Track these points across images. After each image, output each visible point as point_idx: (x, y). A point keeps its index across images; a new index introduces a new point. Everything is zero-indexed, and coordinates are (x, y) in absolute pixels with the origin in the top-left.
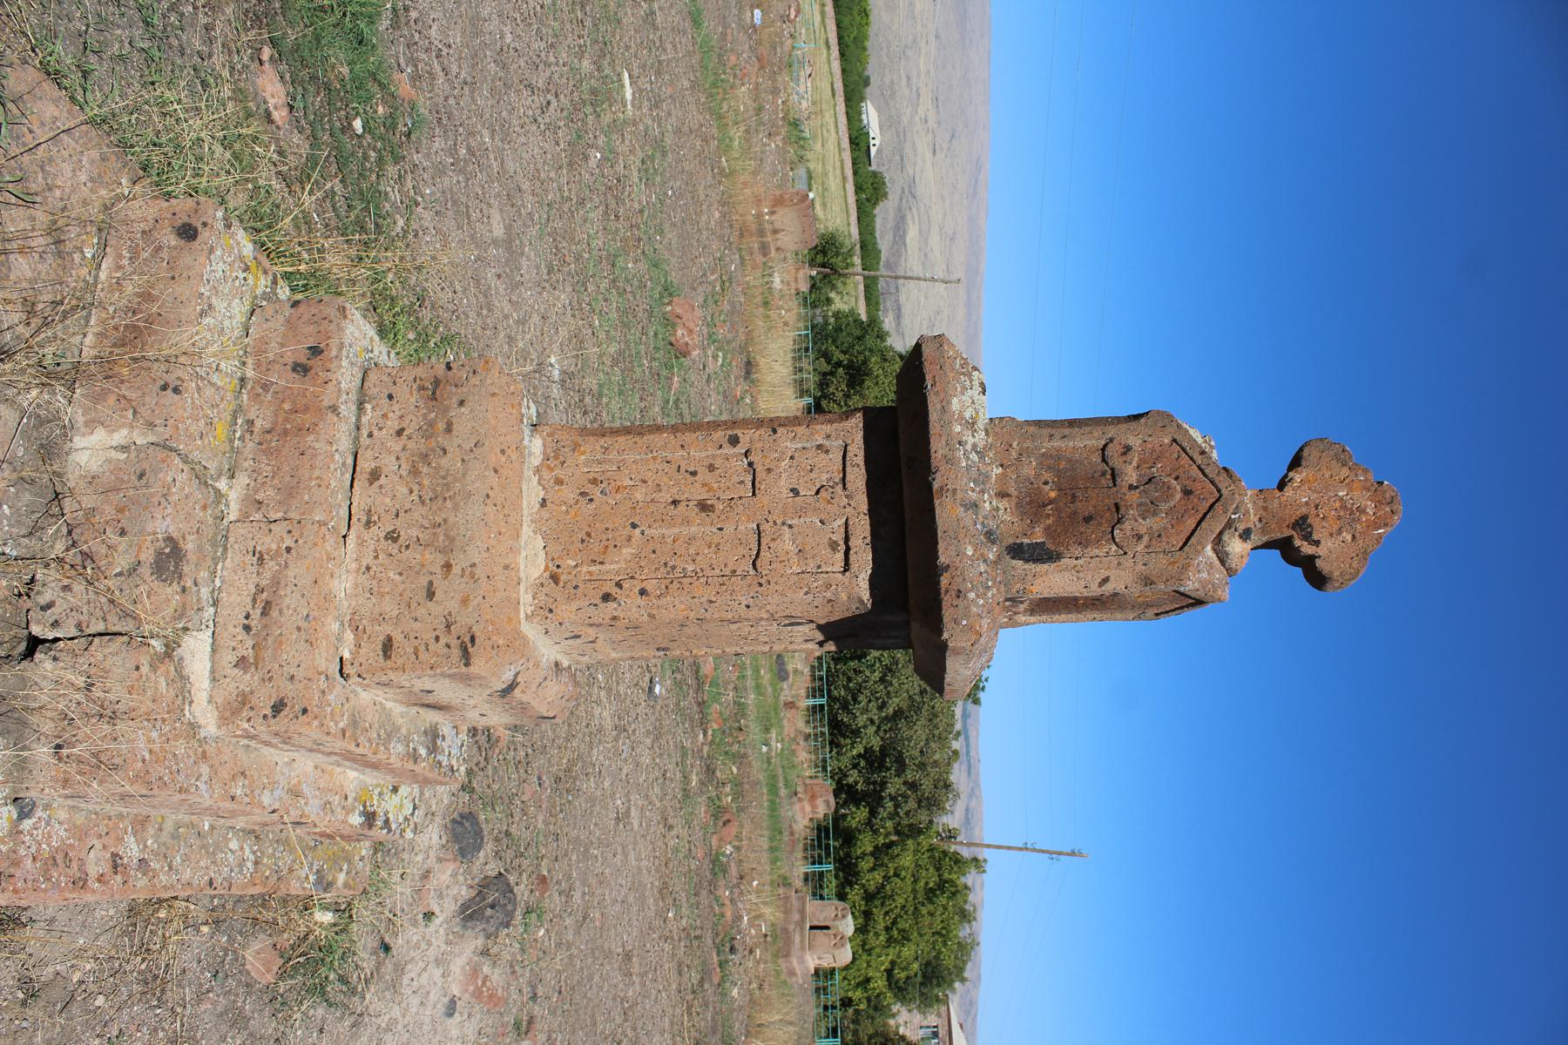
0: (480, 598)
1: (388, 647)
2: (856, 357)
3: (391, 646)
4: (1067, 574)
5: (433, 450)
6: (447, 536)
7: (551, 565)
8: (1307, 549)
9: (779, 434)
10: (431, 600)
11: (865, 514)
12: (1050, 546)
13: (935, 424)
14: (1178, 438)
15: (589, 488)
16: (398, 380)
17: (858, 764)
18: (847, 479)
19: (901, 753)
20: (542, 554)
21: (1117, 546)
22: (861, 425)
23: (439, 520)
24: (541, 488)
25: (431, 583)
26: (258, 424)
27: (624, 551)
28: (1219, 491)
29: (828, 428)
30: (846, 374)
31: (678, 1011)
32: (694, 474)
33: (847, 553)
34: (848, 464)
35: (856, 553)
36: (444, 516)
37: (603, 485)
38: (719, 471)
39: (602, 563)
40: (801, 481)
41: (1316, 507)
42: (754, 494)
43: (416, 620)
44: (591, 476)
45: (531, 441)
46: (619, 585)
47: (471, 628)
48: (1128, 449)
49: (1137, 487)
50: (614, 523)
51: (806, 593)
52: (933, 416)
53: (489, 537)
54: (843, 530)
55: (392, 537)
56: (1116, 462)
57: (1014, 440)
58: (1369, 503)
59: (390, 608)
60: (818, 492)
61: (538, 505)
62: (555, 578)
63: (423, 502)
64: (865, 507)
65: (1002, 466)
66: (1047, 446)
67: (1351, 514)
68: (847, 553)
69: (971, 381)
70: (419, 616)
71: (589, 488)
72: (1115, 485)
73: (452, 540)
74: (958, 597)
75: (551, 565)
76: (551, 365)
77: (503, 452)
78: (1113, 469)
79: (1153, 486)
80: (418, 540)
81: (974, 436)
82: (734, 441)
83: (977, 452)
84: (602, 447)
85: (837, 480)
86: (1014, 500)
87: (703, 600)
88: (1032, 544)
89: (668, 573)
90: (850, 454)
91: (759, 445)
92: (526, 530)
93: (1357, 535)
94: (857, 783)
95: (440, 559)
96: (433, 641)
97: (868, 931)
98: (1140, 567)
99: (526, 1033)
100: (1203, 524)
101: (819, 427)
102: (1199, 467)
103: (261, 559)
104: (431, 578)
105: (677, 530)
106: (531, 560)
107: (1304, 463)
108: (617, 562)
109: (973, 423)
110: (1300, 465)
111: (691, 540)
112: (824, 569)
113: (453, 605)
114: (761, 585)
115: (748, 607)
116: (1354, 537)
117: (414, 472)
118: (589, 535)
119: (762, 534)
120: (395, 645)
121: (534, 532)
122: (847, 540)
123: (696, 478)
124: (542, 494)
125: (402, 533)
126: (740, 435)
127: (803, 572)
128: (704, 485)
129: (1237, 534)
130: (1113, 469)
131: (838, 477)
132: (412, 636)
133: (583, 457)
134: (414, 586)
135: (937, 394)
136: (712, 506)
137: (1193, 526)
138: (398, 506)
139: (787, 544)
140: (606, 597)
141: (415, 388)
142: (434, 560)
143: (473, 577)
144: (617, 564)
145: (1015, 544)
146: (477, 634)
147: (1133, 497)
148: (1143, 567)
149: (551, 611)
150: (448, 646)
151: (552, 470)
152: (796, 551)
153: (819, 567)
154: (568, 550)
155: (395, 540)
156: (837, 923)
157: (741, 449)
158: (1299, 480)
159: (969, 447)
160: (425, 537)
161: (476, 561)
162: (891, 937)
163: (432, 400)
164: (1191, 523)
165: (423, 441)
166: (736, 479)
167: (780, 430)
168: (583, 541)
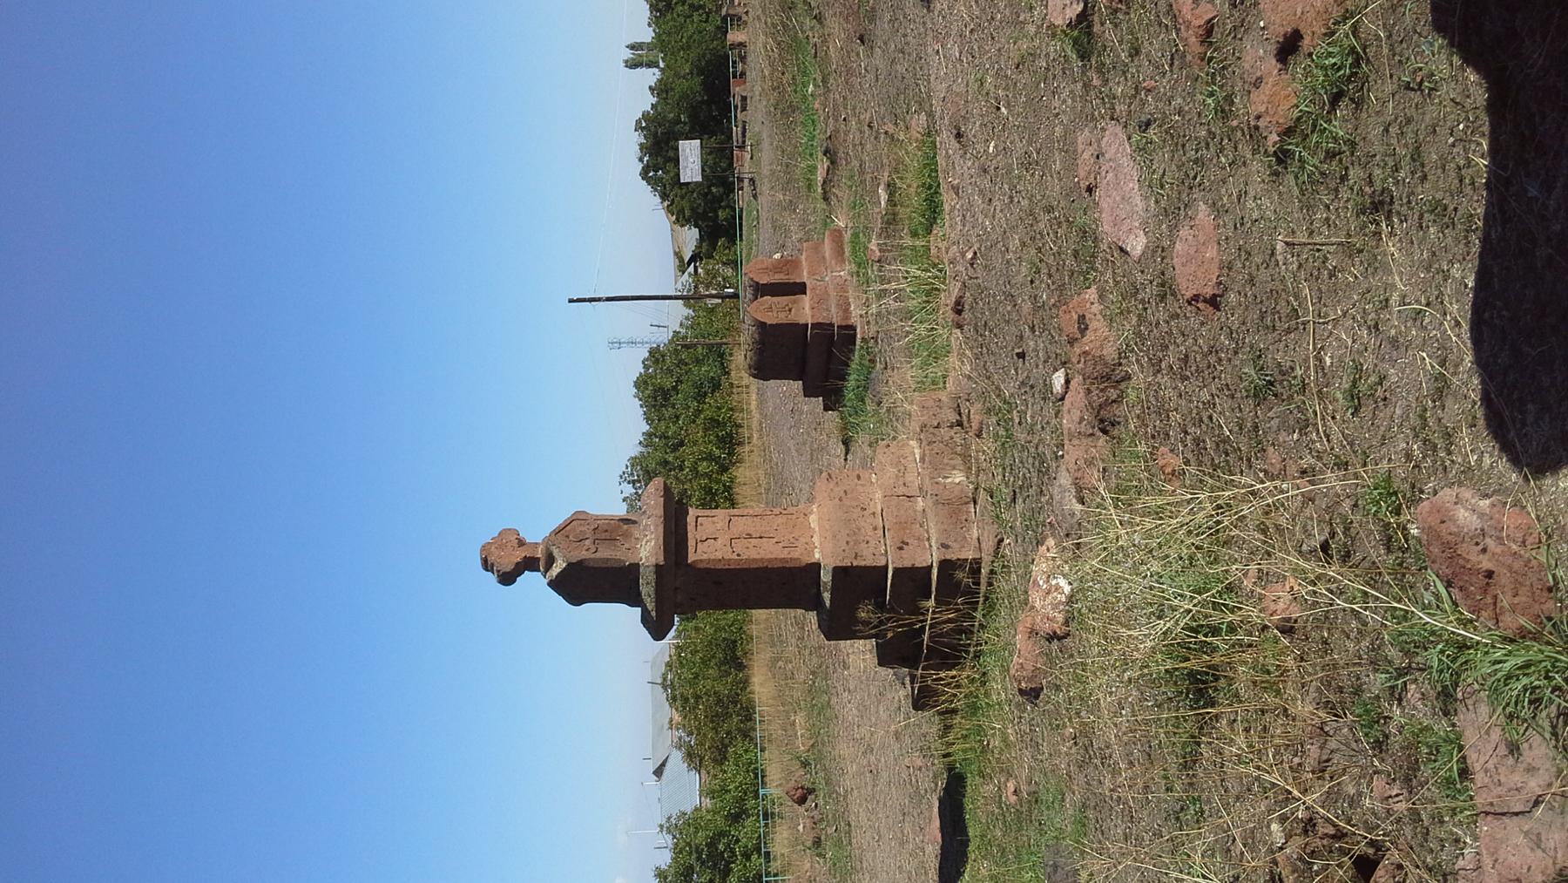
12: (621, 524)
15: (795, 542)
26: (918, 526)
29: (702, 558)
48: (587, 550)
52: (662, 538)
59: (860, 489)
64: (689, 534)
82: (738, 555)
92: (817, 529)
103: (904, 484)
106: (813, 519)
117: (859, 530)
122: (696, 526)
131: (699, 544)
142: (847, 502)
155: (862, 508)
164: (568, 527)
167: (720, 557)
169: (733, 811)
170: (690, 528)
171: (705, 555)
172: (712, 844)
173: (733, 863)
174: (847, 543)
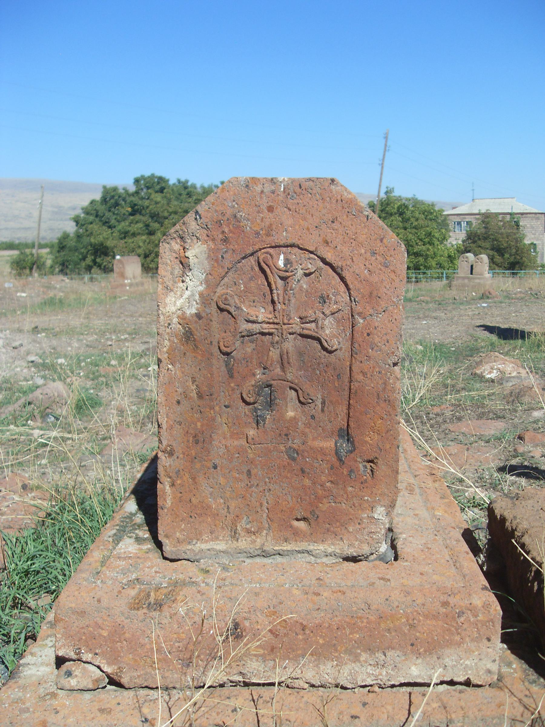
2: (89, 251)
30: (100, 257)
97: (427, 255)
156: (470, 261)
162: (429, 243)
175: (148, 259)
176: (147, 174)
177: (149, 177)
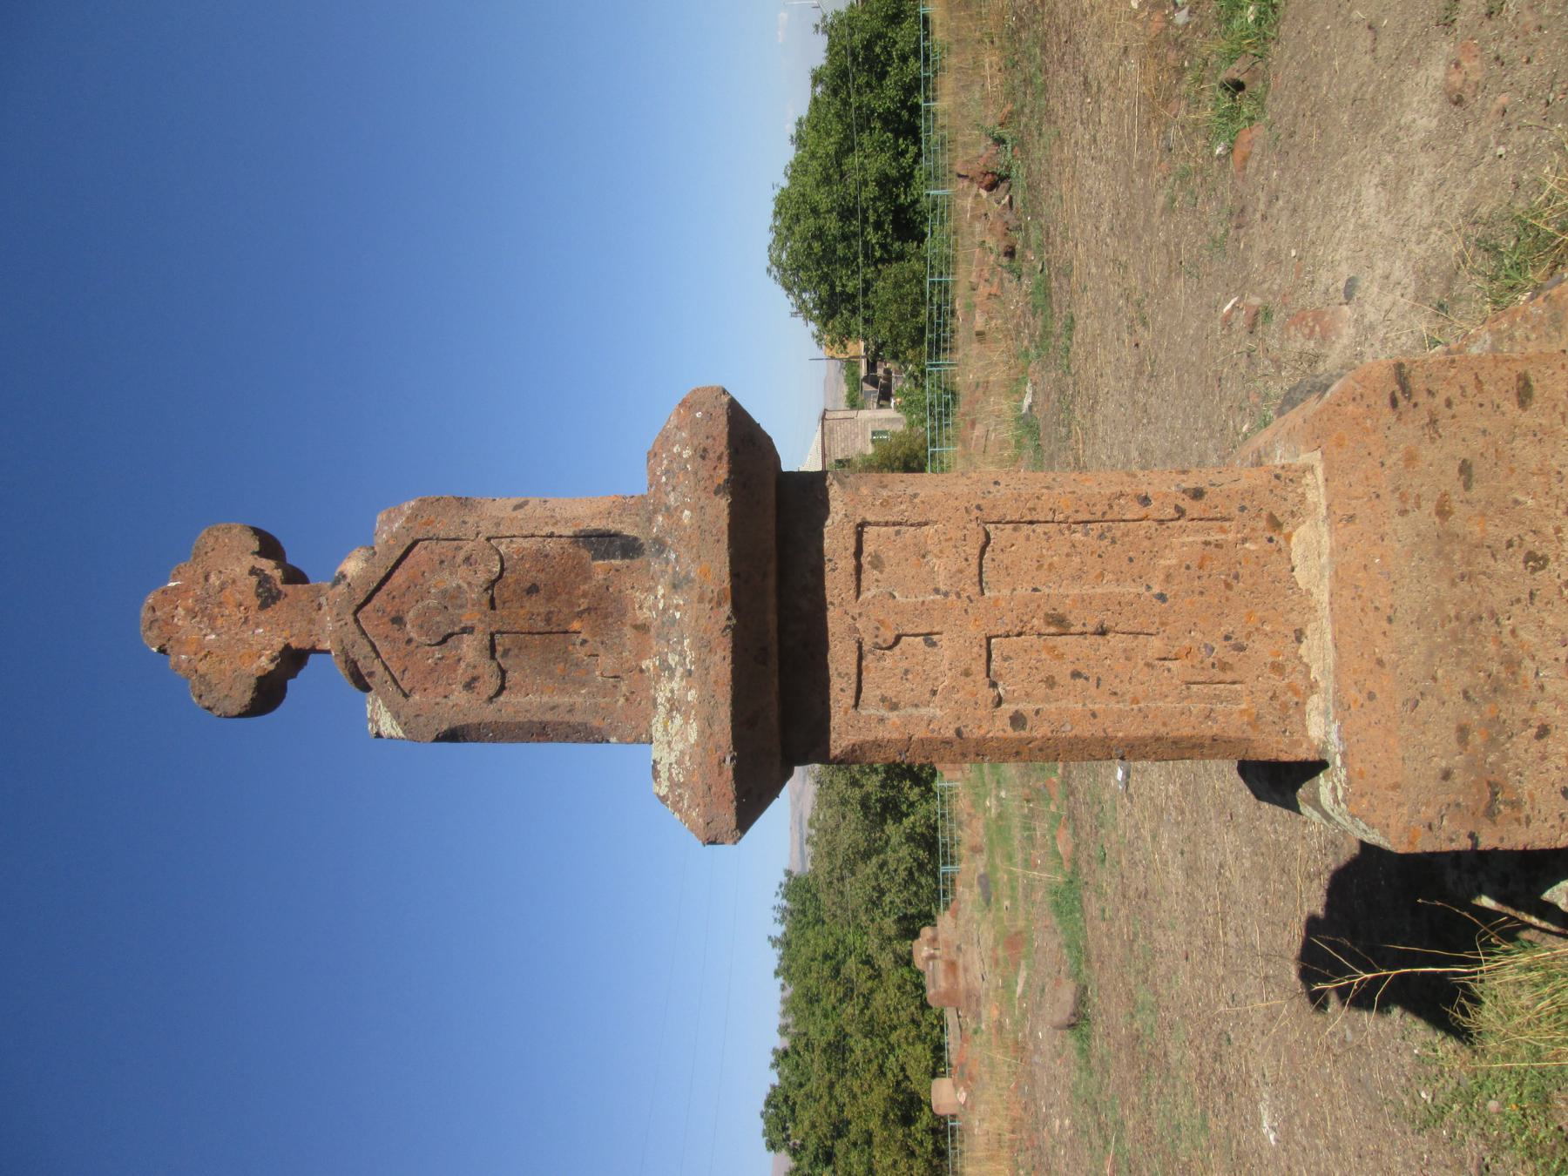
0: (1389, 462)
1: (1524, 393)
3: (1519, 394)
4: (568, 515)
5: (1485, 699)
6: (1448, 558)
7: (1282, 543)
8: (267, 565)
9: (952, 727)
10: (1464, 461)
11: (832, 604)
12: (586, 554)
13: (722, 700)
14: (400, 698)
15: (1231, 657)
16: (1557, 822)
17: (909, 807)
18: (855, 656)
19: (866, 816)
20: (1296, 559)
21: (497, 550)
22: (833, 736)
23: (1464, 585)
24: (1305, 660)
25: (1467, 486)
27: (1174, 562)
28: (357, 621)
29: (881, 733)
31: (1088, 453)
32: (1076, 675)
33: (858, 552)
34: (854, 678)
35: (846, 549)
36: (1457, 591)
37: (1211, 660)
38: (1038, 678)
39: (1207, 543)
40: (921, 657)
41: (246, 620)
42: (989, 639)
43: (1484, 432)
44: (1229, 676)
45: (1327, 733)
46: (1181, 512)
47: (1399, 419)
49: (464, 630)
50: (1192, 603)
51: (915, 496)
52: (724, 713)
53: (1382, 557)
54: (864, 584)
55: (1536, 561)
56: (488, 670)
57: (622, 707)
58: (180, 623)
59: (1529, 453)
60: (898, 639)
61: (1308, 633)
62: (1274, 523)
63: (1493, 614)
65: (642, 671)
66: (580, 698)
67: (203, 611)
68: (858, 552)
69: (670, 778)
70: (1481, 440)
71: (1231, 657)
72: (492, 635)
73: (1439, 553)
74: (705, 450)
75: (1282, 543)
76: (1273, 1129)
77: (1371, 696)
78: (493, 657)
79: (442, 629)
80: (1493, 556)
81: (672, 691)
82: (1017, 720)
83: (669, 668)
84: (1215, 721)
85: (870, 657)
86: (628, 619)
87: (1057, 490)
88: (609, 558)
89: (1110, 529)
90: (851, 692)
91: (982, 712)
92: (1322, 595)
93: (202, 580)
94: (911, 788)
95: (1456, 523)
96: (1456, 401)
98: (471, 520)
99: (1257, 314)
100: (382, 574)
101: (895, 736)
102: (378, 656)
104: (1468, 495)
105: (1099, 590)
107: (253, 681)
108: (1183, 544)
109: (671, 710)
110: (260, 679)
111: (1078, 577)
112: (892, 530)
113: (1428, 453)
114: (979, 507)
115: (996, 483)
116: (207, 578)
117: (1512, 664)
118: (1228, 586)
119: (976, 579)
120: (1512, 395)
121: (1309, 592)
122: (859, 569)
123: (1071, 668)
124: (1303, 650)
125: (1521, 566)
126: (1009, 729)
127: (920, 525)
128: (1060, 657)
129: (348, 580)
130: (493, 657)
132: (1488, 409)
133: (1243, 706)
134: (1494, 483)
135: (718, 747)
136: (1049, 624)
137: (397, 573)
138: (1533, 610)
139: (942, 567)
140: (1197, 494)
141: (1527, 807)
142: (1465, 522)
143: (1402, 495)
144: (1185, 542)
145: (632, 558)
146: (1387, 410)
147: (469, 617)
148: (467, 519)
149: (1277, 477)
150: (1430, 393)
151: (1290, 687)
152: (929, 557)
153: (898, 533)
154: (1257, 564)
155: (1531, 556)
157: (1008, 708)
158: (263, 658)
159: (680, 671)
160: (1484, 560)
161: (1398, 519)
163: (1497, 785)
164: (399, 578)
165: (1503, 716)
166: (1016, 664)
167: (950, 733)
168: (1236, 577)
169: (890, 12)
170: (836, 583)
171: (893, 717)
172: (868, 46)
173: (890, 66)
174: (1463, 732)
175: (918, 1150)
176: (760, 1125)
177: (766, 1123)
